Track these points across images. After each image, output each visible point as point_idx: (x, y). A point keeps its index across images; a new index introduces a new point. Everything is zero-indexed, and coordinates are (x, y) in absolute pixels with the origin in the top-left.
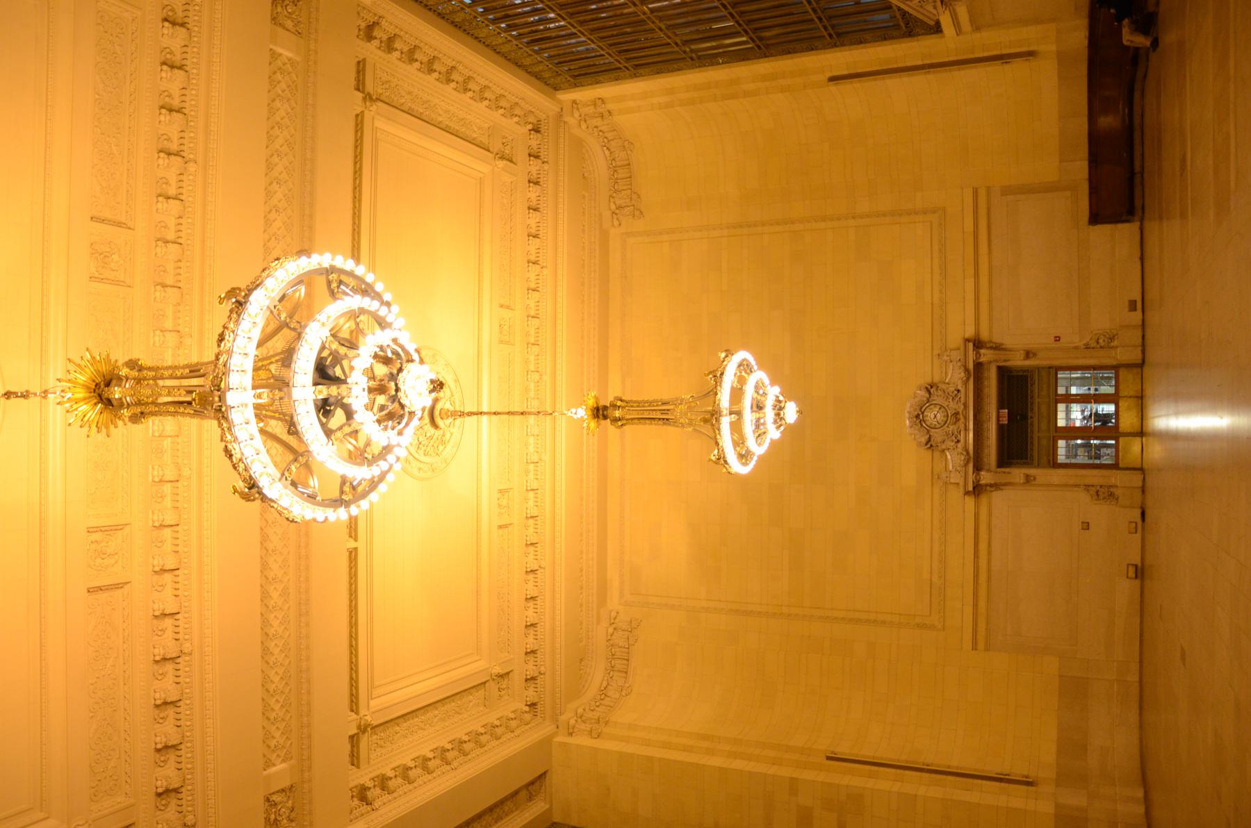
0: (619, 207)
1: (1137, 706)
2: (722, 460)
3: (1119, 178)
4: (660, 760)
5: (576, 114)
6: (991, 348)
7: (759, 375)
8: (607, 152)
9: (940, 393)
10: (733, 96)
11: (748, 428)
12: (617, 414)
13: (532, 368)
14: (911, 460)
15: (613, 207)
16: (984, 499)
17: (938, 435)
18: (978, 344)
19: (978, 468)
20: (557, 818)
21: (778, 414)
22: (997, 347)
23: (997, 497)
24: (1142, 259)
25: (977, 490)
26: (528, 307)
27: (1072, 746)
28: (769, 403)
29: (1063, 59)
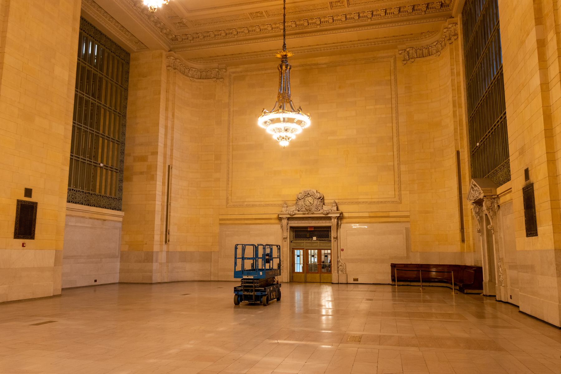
0: (408, 53)
1: (202, 279)
3: (408, 276)
4: (160, 98)
5: (450, 26)
6: (338, 224)
7: (299, 130)
8: (435, 44)
9: (319, 203)
10: (454, 106)
11: (277, 125)
12: (284, 67)
13: (310, 21)
14: (291, 192)
15: (408, 50)
16: (277, 221)
17: (301, 203)
18: (340, 218)
19: (288, 219)
20: (132, 56)
21: (283, 138)
22: (338, 226)
23: (279, 227)
24: (373, 284)
25: (280, 219)
26: (351, 14)
27: (185, 257)
28: (288, 134)
29: (462, 253)
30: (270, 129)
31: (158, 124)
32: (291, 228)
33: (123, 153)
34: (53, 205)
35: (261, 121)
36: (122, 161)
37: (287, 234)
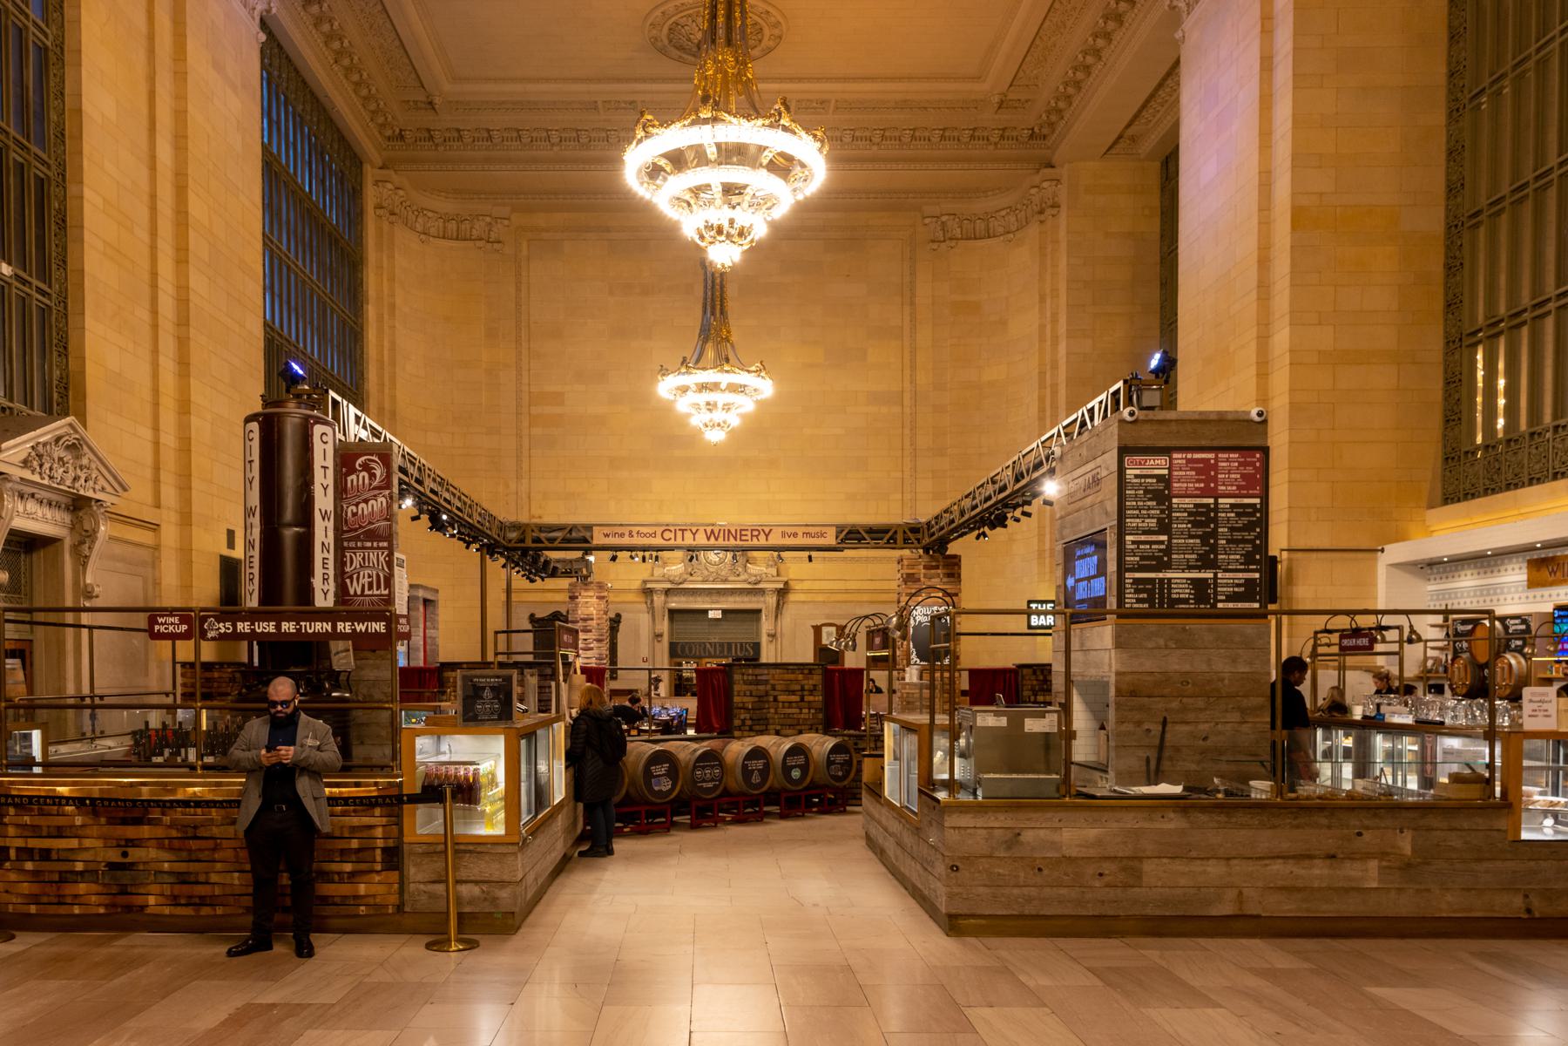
18: (783, 593)
19: (667, 592)
22: (779, 608)
32: (672, 612)
35: (666, 387)
37: (664, 626)
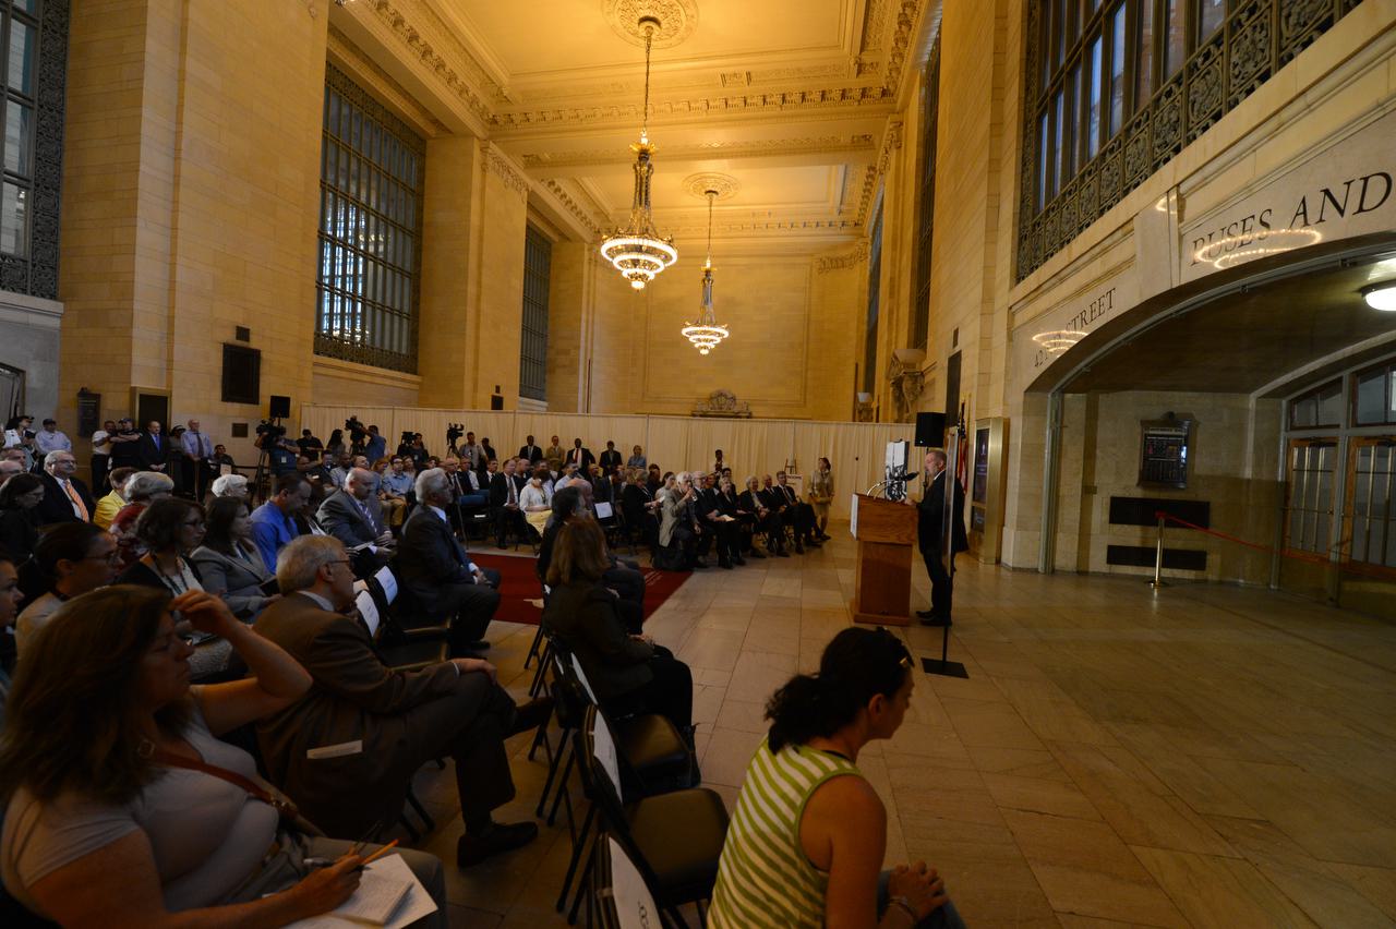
2: (687, 326)
7: (718, 340)
10: (858, 322)
30: (692, 339)
31: (580, 320)
33: (545, 345)
34: (511, 396)
36: (545, 354)
